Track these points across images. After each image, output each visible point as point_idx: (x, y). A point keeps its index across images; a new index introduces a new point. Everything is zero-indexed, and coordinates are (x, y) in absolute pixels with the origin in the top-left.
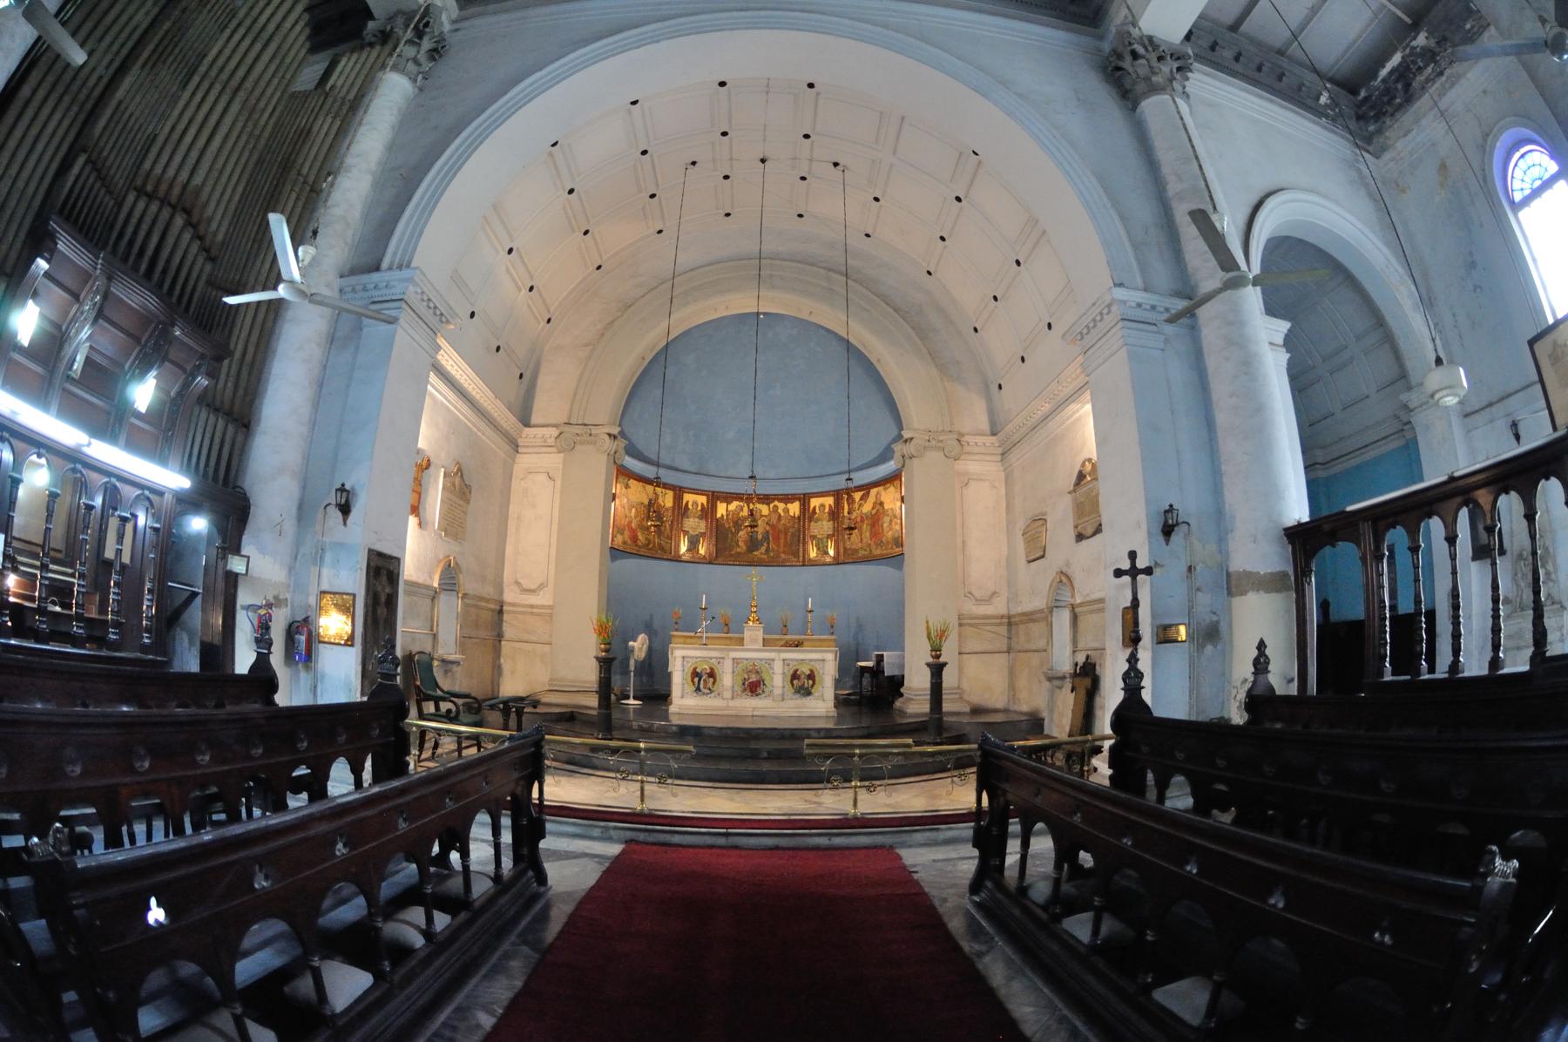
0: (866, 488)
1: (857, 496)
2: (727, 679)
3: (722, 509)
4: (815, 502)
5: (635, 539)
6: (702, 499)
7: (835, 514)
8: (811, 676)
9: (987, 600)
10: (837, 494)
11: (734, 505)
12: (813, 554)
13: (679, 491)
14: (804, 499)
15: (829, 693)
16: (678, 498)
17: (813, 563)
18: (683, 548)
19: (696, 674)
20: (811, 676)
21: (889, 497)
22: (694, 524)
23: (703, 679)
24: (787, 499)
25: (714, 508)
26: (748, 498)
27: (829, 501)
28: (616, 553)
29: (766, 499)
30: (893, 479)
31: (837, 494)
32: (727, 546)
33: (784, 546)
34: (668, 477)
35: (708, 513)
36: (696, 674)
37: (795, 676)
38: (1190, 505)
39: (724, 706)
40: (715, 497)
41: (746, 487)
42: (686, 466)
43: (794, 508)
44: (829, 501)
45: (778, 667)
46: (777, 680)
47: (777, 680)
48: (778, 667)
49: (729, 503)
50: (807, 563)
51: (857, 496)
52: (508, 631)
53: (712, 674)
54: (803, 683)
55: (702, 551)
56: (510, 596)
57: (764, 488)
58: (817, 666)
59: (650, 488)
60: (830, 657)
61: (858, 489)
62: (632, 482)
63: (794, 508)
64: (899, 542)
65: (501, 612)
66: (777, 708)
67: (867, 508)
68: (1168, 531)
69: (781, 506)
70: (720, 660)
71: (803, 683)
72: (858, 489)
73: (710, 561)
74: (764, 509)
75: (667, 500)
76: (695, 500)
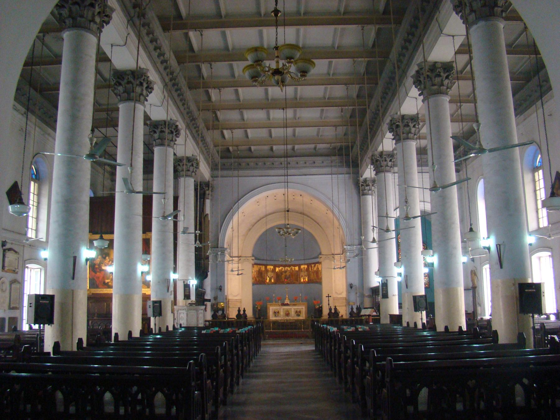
0: (315, 264)
1: (313, 265)
2: (282, 313)
3: (277, 269)
4: (302, 267)
5: (256, 280)
6: (272, 267)
7: (307, 270)
8: (300, 312)
9: (340, 294)
10: (309, 265)
11: (280, 268)
12: (302, 280)
13: (266, 266)
14: (299, 266)
15: (304, 316)
16: (266, 268)
17: (302, 283)
18: (268, 281)
19: (275, 312)
20: (300, 312)
21: (320, 266)
22: (270, 274)
23: (276, 313)
24: (295, 266)
25: (275, 269)
26: (285, 266)
27: (306, 266)
28: (253, 284)
29: (289, 266)
30: (319, 263)
31: (309, 265)
32: (279, 279)
33: (293, 278)
34: (264, 262)
35: (274, 271)
36: (275, 312)
37: (296, 312)
38: (356, 282)
39: (281, 317)
40: (275, 266)
41: (284, 263)
42: (268, 259)
43: (297, 268)
44: (306, 266)
45: (293, 310)
46: (293, 313)
47: (293, 313)
48: (293, 310)
49: (279, 267)
50: (301, 283)
51: (313, 265)
52: (231, 306)
53: (278, 312)
54: (298, 313)
55: (273, 281)
56: (230, 297)
57: (287, 263)
58: (301, 310)
59: (259, 266)
60: (304, 307)
61: (313, 263)
62: (255, 266)
63: (297, 268)
64: (321, 278)
65: (228, 301)
66: (293, 317)
67: (315, 269)
68: (351, 287)
69: (293, 268)
70: (280, 309)
71: (298, 313)
72: (313, 263)
73: (275, 283)
74: (289, 269)
75: (263, 268)
76: (270, 267)
